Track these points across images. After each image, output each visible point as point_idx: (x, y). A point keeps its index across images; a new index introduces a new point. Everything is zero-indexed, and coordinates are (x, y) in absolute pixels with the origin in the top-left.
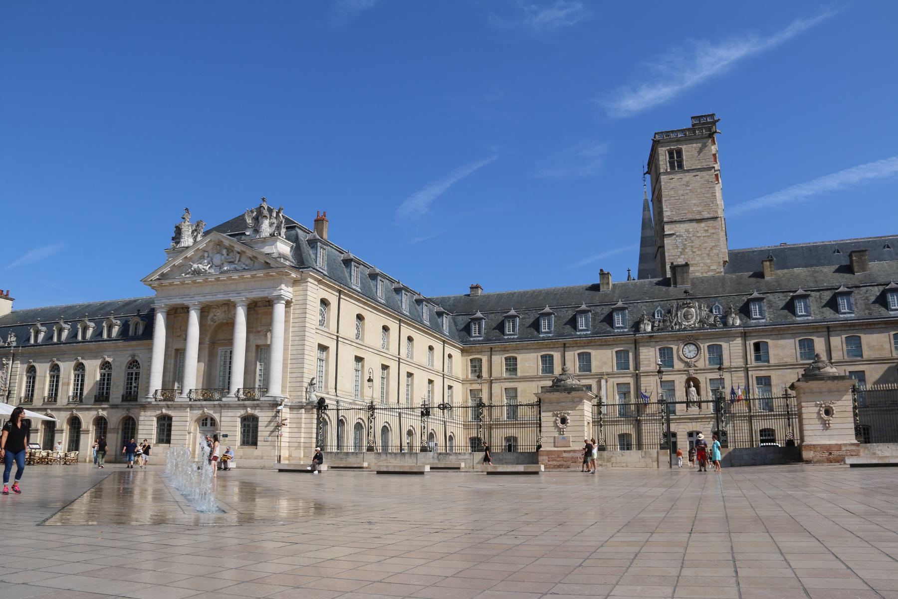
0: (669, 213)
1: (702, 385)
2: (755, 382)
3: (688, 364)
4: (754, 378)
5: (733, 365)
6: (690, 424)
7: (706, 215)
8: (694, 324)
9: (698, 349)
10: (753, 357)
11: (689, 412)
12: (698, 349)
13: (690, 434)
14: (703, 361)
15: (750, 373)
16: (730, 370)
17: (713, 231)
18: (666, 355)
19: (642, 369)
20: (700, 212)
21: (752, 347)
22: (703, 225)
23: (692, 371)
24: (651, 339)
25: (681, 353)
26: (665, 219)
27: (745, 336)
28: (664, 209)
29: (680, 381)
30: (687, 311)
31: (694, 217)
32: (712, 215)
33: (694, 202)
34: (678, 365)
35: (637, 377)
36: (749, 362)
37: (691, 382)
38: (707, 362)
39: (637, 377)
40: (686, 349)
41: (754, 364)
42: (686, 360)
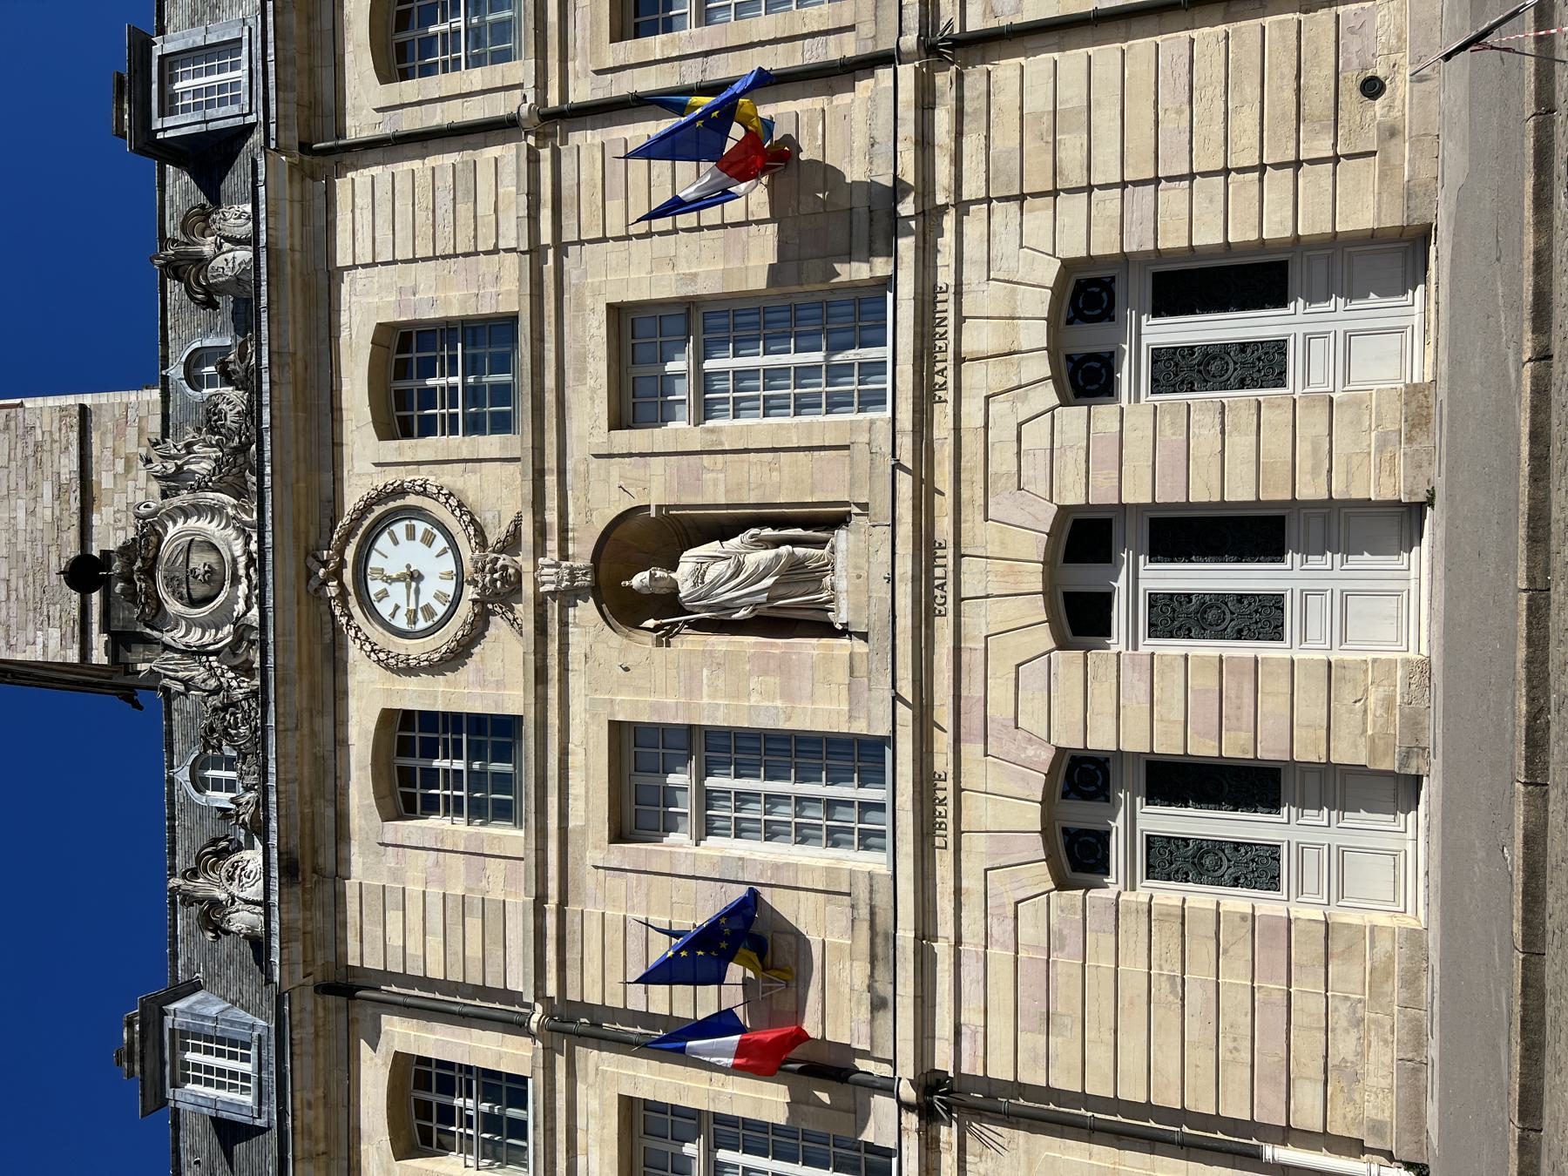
0: (55, 633)
1: (657, 487)
2: (656, 45)
3: (500, 594)
4: (630, 50)
5: (513, 233)
6: (978, 620)
7: (71, 463)
8: (242, 531)
9: (391, 508)
10: (476, 78)
11: (873, 617)
12: (391, 508)
13: (1081, 618)
14: (484, 476)
15: (583, 91)
16: (544, 258)
17: (132, 432)
18: (453, 761)
19: (518, 980)
20: (60, 492)
21: (410, 89)
22: (103, 479)
23: (539, 573)
24: (312, 872)
25: (416, 649)
26: (73, 656)
27: (322, 151)
28: (33, 654)
29: (624, 676)
30: (169, 581)
31: (75, 520)
32: (74, 436)
33: (21, 515)
34: (494, 682)
35: (575, 1027)
36: (498, 107)
37: (633, 572)
38: (490, 444)
39: (575, 1027)
40: (394, 601)
41: (521, 70)
42: (465, 610)
